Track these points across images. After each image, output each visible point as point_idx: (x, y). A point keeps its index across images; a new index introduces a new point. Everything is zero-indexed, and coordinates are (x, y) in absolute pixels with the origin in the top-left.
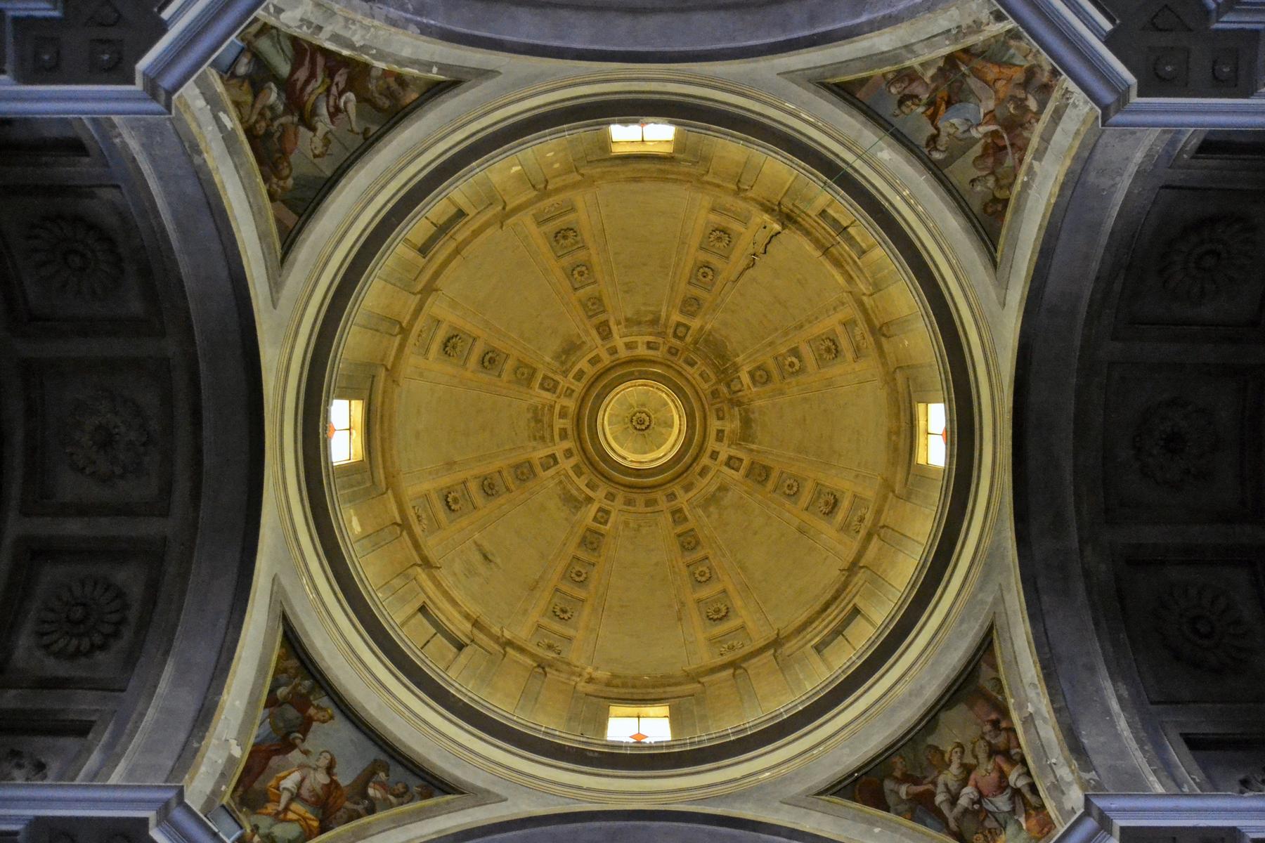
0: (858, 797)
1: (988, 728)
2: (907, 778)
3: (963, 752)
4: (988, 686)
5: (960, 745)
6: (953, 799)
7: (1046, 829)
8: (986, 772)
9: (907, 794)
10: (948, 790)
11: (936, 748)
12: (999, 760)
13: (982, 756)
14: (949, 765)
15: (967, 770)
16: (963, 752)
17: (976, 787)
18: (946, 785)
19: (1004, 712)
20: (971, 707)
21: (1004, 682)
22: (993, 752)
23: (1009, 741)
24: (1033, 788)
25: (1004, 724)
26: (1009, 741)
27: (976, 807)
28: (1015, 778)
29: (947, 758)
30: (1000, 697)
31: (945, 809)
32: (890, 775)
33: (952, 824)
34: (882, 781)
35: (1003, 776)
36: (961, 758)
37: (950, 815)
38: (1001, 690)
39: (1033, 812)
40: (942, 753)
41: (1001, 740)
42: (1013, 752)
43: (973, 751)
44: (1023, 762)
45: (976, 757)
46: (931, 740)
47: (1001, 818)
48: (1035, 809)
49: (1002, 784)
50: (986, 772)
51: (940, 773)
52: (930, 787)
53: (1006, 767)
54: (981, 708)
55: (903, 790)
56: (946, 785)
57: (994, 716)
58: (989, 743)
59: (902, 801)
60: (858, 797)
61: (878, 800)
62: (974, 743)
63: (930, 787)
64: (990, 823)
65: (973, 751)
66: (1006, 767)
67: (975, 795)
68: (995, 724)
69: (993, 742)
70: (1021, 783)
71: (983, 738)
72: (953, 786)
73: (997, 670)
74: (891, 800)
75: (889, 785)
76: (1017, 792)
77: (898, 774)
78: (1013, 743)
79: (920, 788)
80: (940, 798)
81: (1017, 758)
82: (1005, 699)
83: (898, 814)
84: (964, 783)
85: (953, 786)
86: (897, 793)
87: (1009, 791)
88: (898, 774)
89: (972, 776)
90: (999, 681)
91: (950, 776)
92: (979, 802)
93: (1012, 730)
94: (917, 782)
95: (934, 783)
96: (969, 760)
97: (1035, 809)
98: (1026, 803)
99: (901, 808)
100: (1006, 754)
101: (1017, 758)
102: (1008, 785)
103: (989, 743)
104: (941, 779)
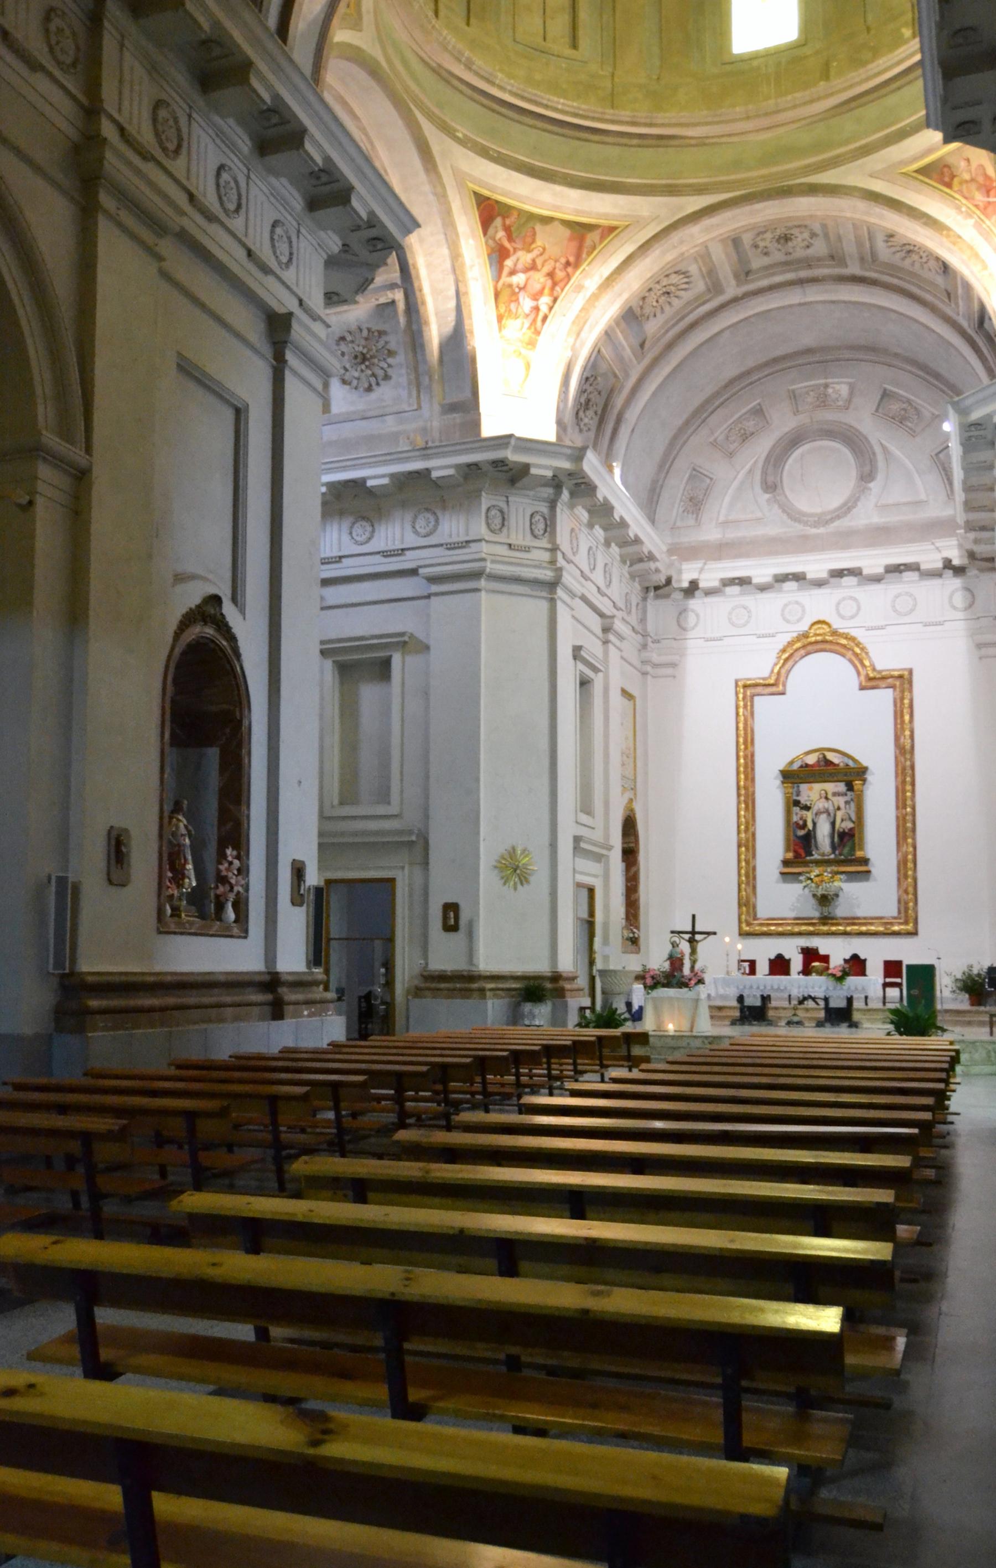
0: (482, 207)
1: (563, 260)
2: (507, 229)
3: (541, 254)
4: (588, 242)
5: (544, 249)
6: (513, 273)
7: (530, 347)
8: (539, 279)
9: (500, 239)
10: (515, 265)
11: (534, 234)
12: (549, 283)
13: (546, 269)
14: (529, 251)
15: (533, 267)
16: (541, 254)
17: (527, 280)
18: (518, 260)
19: (577, 265)
20: (571, 239)
21: (595, 253)
22: (551, 275)
23: (561, 281)
24: (545, 318)
25: (570, 270)
26: (561, 281)
27: (517, 290)
28: (545, 301)
29: (533, 246)
30: (584, 256)
31: (506, 271)
32: (504, 218)
33: (500, 285)
34: (499, 215)
35: (541, 292)
36: (538, 256)
37: (505, 279)
38: (589, 254)
39: (533, 329)
40: (534, 241)
41: (560, 274)
42: (558, 289)
43: (545, 261)
44: (555, 300)
45: (543, 266)
46: (538, 227)
47: (520, 310)
48: (535, 329)
49: (536, 297)
50: (539, 279)
51: (523, 249)
52: (512, 250)
53: (546, 291)
54: (574, 244)
55: (501, 234)
56: (518, 260)
57: (572, 259)
58: (554, 269)
59: (494, 239)
60: (482, 207)
61: (486, 223)
62: (550, 258)
63: (512, 250)
64: (513, 306)
65: (545, 261)
66: (546, 291)
67: (522, 285)
68: (568, 264)
69: (557, 271)
70: (544, 309)
71: (556, 261)
72: (520, 266)
73: (601, 242)
74: (491, 231)
75: (498, 222)
76: (537, 309)
77: (508, 222)
78: (562, 284)
79: (507, 244)
80: (509, 263)
81: (555, 294)
82: (586, 260)
83: (486, 243)
84: (526, 270)
85: (520, 266)
86: (496, 232)
87: (533, 304)
88: (508, 222)
89: (531, 273)
90: (594, 248)
91: (525, 258)
92: (520, 289)
93: (568, 277)
94: (510, 238)
95: (515, 250)
96: (539, 262)
97: (535, 329)
98: (534, 321)
99: (491, 242)
100: (555, 284)
101: (555, 294)
102: (537, 300)
103: (554, 269)
104: (520, 254)
